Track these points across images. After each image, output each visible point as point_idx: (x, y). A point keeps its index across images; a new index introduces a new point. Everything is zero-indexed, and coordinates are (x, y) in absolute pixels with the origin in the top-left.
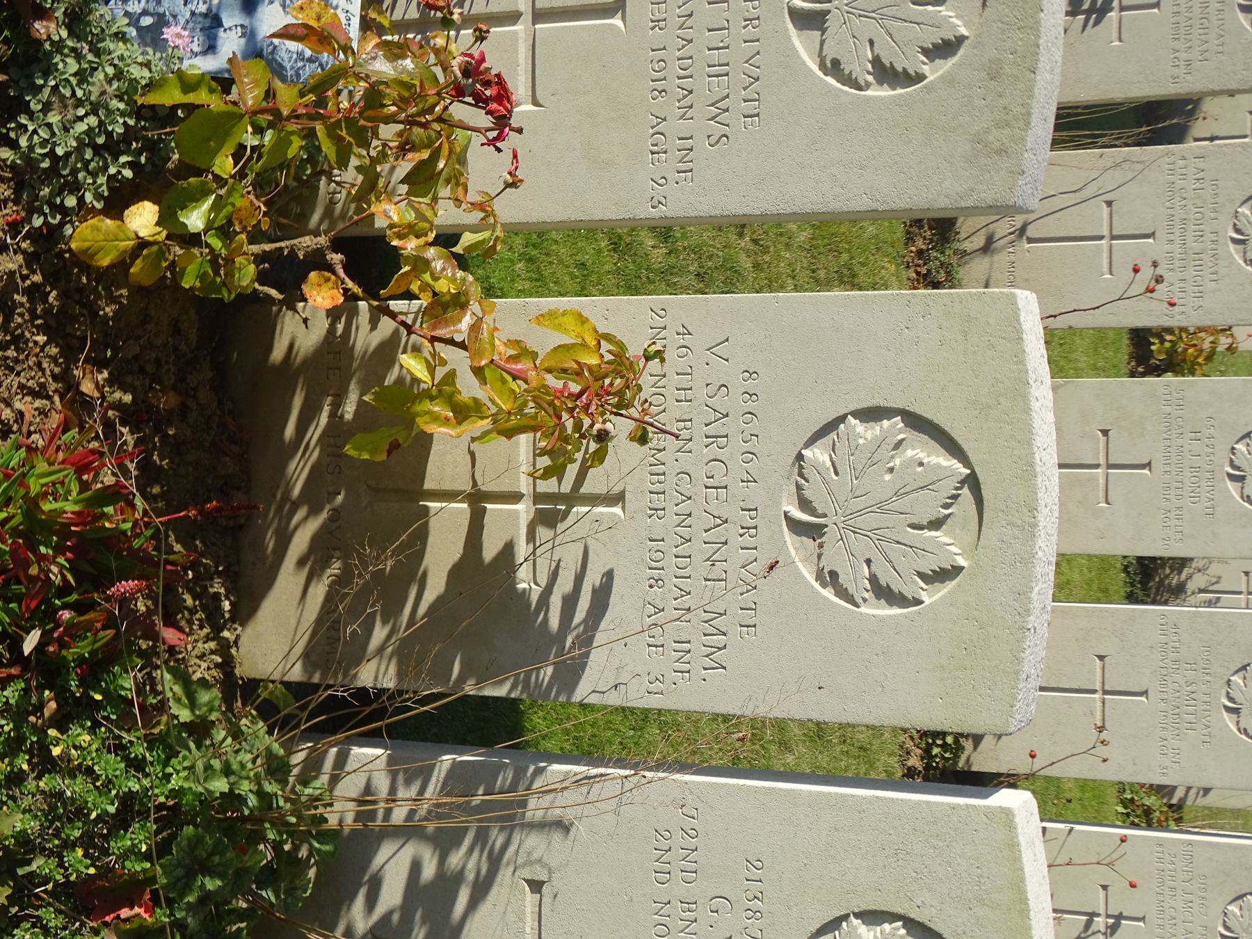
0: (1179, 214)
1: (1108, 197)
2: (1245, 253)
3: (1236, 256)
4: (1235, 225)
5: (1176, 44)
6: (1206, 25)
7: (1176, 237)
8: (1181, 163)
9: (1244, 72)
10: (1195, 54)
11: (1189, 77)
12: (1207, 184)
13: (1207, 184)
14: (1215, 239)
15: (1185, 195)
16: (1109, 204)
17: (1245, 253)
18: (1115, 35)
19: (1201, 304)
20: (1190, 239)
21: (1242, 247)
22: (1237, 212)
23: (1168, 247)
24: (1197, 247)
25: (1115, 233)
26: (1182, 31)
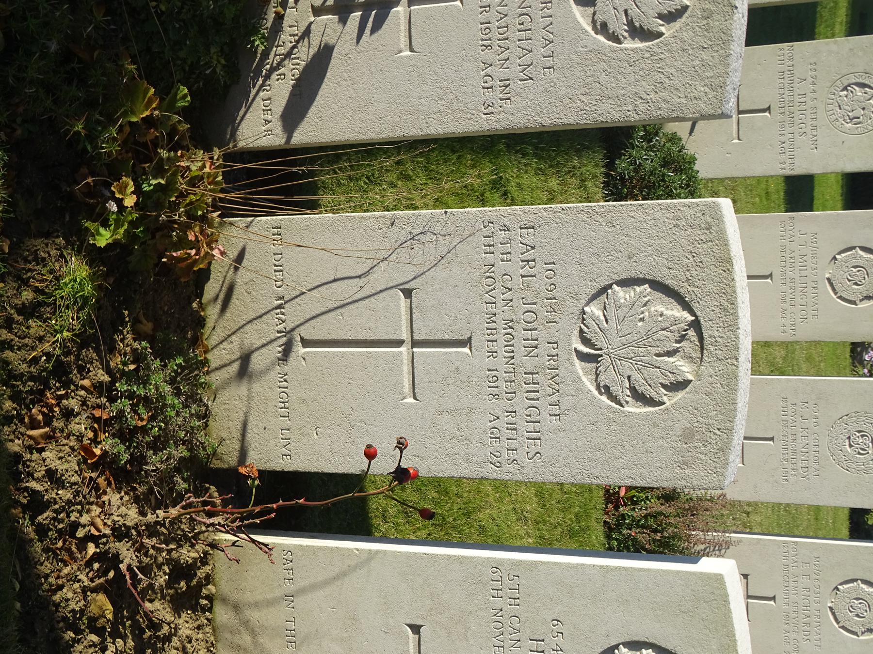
0: (503, 314)
1: (406, 286)
2: (597, 375)
3: (584, 379)
4: (581, 331)
5: (487, 55)
6: (527, 25)
7: (500, 346)
8: (502, 235)
9: (583, 98)
10: (514, 71)
11: (507, 105)
12: (540, 268)
13: (540, 268)
14: (555, 352)
15: (509, 285)
16: (408, 293)
17: (597, 375)
18: (403, 40)
19: (539, 449)
20: (519, 351)
21: (592, 366)
22: (584, 312)
23: (490, 362)
24: (531, 364)
25: (416, 337)
26: (495, 34)
